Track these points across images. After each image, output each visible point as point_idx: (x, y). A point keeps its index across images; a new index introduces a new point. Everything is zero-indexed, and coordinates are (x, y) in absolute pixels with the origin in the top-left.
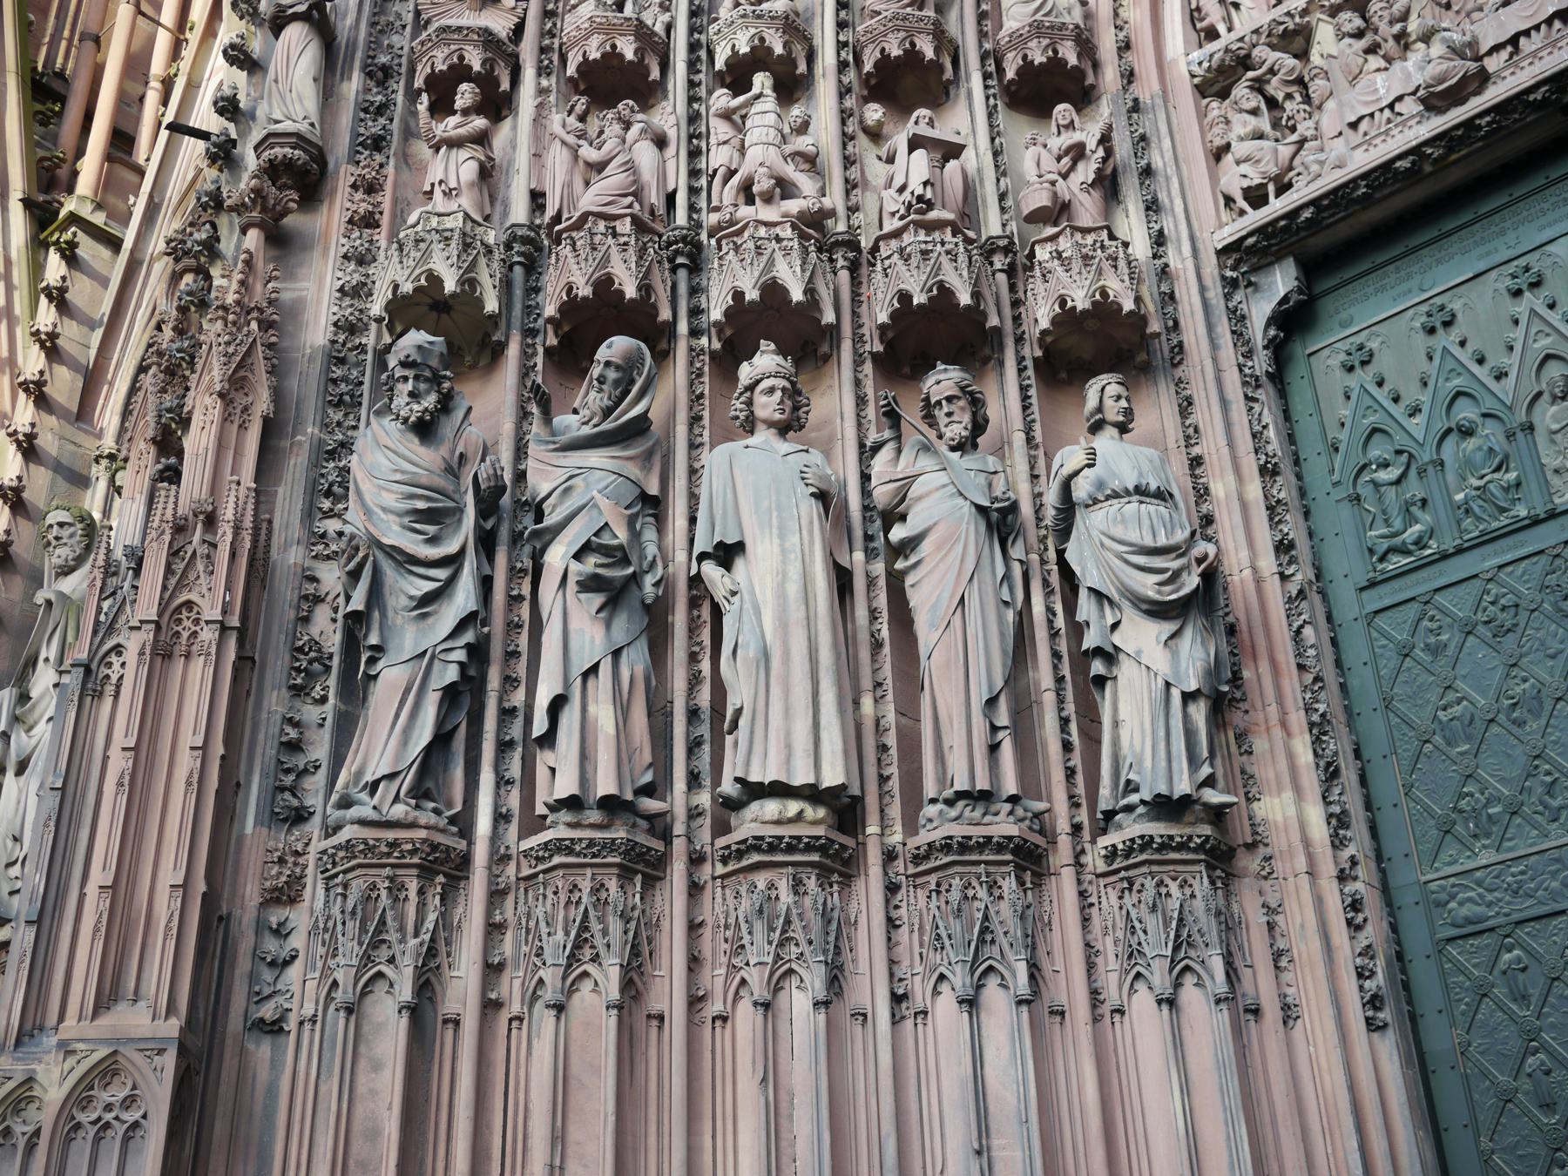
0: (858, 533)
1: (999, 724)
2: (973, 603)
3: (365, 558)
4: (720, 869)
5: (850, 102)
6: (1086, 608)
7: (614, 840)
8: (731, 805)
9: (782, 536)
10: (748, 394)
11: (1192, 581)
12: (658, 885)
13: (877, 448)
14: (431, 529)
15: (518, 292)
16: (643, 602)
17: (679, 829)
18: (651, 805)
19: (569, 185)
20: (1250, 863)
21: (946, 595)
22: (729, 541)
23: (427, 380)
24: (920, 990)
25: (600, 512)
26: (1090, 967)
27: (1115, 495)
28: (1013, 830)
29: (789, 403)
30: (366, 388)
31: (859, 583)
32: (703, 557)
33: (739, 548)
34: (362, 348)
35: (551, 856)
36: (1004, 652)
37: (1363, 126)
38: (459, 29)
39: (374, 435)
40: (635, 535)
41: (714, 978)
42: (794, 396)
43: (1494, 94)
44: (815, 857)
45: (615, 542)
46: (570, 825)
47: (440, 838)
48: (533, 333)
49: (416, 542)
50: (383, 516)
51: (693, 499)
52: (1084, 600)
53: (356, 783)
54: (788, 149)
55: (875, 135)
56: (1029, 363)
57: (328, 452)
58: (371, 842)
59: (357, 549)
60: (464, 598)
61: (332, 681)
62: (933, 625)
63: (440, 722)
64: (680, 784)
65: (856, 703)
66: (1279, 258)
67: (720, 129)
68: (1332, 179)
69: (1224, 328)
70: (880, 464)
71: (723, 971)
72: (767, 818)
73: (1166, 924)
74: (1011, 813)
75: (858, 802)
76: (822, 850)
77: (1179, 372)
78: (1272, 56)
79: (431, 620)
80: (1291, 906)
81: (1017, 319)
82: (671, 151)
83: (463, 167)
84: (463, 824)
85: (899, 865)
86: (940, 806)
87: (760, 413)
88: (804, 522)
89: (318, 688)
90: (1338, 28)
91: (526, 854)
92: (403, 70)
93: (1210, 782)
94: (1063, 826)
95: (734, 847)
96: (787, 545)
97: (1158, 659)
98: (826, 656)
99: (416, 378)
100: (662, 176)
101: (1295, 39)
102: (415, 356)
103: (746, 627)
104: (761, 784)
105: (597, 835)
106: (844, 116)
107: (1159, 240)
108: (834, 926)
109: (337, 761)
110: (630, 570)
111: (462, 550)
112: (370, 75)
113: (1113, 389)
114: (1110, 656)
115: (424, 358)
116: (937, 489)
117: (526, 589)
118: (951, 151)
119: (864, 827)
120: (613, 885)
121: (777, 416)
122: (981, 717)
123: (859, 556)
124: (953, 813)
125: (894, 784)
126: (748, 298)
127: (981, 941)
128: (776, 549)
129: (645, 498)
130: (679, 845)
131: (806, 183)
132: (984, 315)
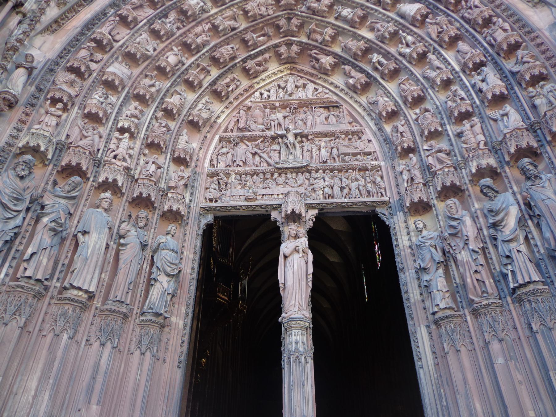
4: (57, 302)
5: (143, 147)
6: (154, 269)
8: (65, 288)
11: (176, 272)
12: (40, 301)
13: (124, 222)
14: (16, 202)
15: (56, 155)
17: (51, 290)
18: (46, 283)
19: (77, 137)
20: (166, 329)
24: (92, 340)
26: (130, 343)
27: (168, 249)
28: (125, 311)
31: (110, 249)
32: (79, 232)
37: (234, 197)
38: (64, 91)
41: (47, 326)
43: (257, 203)
44: (81, 305)
46: (26, 282)
51: (80, 217)
52: (154, 266)
54: (128, 152)
55: (144, 155)
60: (18, 221)
62: (124, 263)
65: (101, 274)
66: (211, 213)
67: (114, 141)
68: (226, 204)
69: (197, 222)
70: (124, 225)
71: (49, 325)
73: (148, 338)
75: (94, 296)
76: (83, 304)
77: (186, 228)
78: (223, 176)
80: (171, 340)
82: (102, 140)
83: (53, 121)
85: (97, 311)
90: (236, 177)
91: (10, 286)
92: (46, 91)
93: (166, 312)
97: (165, 285)
100: (98, 145)
101: (228, 175)
102: (28, 161)
105: (32, 287)
106: (141, 149)
107: (191, 201)
108: (79, 321)
110: (61, 229)
112: (37, 88)
113: (174, 228)
114: (156, 280)
118: (159, 167)
119: (93, 301)
120: (30, 299)
121: (106, 207)
123: (112, 243)
125: (102, 294)
126: (109, 180)
127: (110, 332)
129: (69, 213)
130: (49, 294)
131: (129, 160)
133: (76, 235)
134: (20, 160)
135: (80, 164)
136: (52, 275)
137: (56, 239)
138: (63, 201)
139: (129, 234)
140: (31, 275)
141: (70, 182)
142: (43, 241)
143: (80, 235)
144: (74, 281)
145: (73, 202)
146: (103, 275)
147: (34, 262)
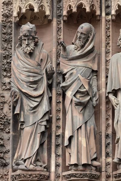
3: (19, 98)
7: (86, 174)
14: (35, 86)
16: (93, 105)
17: (103, 169)
18: (96, 163)
22: (116, 89)
23: (31, 39)
25: (81, 81)
30: (13, 35)
32: (109, 93)
34: (10, 22)
35: (70, 177)
39: (17, 55)
40: (90, 85)
45: (84, 90)
46: (75, 170)
47: (42, 173)
48: (60, 16)
49: (31, 91)
50: (22, 82)
53: (20, 158)
57: (4, 57)
58: (25, 175)
59: (16, 96)
60: (44, 107)
61: (11, 127)
63: (40, 141)
64: (104, 157)
79: (36, 113)
84: (48, 168)
89: (7, 129)
95: (118, 175)
99: (28, 39)
102: (28, 34)
105: (82, 173)
109: (14, 149)
111: (44, 92)
115: (30, 33)
117: (61, 100)
129: (93, 71)
130: (103, 174)
133: (108, 96)
134: (21, 35)
135: (81, 4)
136: (99, 152)
137: (87, 111)
138: (79, 63)
140: (76, 162)
141: (79, 35)
142: (75, 120)
143: (111, 97)
145: (92, 55)
147: (74, 147)
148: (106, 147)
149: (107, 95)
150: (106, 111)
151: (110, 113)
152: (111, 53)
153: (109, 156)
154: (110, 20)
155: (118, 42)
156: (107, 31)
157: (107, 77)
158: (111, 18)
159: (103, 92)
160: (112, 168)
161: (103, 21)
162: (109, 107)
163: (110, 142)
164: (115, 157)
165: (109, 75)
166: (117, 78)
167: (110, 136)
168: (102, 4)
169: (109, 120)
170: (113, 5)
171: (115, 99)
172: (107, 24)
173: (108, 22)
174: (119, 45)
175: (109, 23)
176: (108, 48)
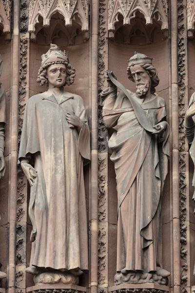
0: (95, 140)
1: (148, 239)
2: (140, 182)
9: (55, 151)
10: (44, 71)
17: (11, 284)
21: (129, 177)
22: (33, 153)
29: (64, 75)
32: (21, 159)
33: (38, 153)
36: (154, 203)
42: (67, 70)
56: (185, 42)
64: (12, 264)
72: (46, 282)
74: (151, 278)
81: (181, 18)
86: (121, 275)
87: (51, 81)
88: (66, 142)
94: (177, 281)
96: (58, 155)
98: (73, 209)
103: (39, 195)
104: (44, 268)
116: (129, 122)
121: (58, 83)
122: (139, 237)
123: (94, 152)
124: (126, 279)
125: (106, 261)
128: (53, 158)
132: (160, 24)
133: (20, 164)
139: (121, 121)
143: (25, 165)
144: (38, 259)
146: (94, 226)
148: (17, 247)
149: (19, 162)
150: (18, 189)
151: (25, 193)
152: (28, 94)
153: (21, 262)
154: (26, 41)
155: (39, 76)
156: (21, 59)
157: (20, 133)
158: (28, 37)
159: (13, 157)
160: (26, 281)
161: (16, 41)
162: (22, 182)
163: (22, 240)
164: (31, 264)
165: (23, 130)
166: (34, 136)
167: (24, 229)
168: (15, 14)
169: (22, 203)
170: (30, 15)
171: (30, 169)
172: (22, 46)
173: (24, 43)
174: (40, 81)
175: (26, 45)
176: (23, 85)
